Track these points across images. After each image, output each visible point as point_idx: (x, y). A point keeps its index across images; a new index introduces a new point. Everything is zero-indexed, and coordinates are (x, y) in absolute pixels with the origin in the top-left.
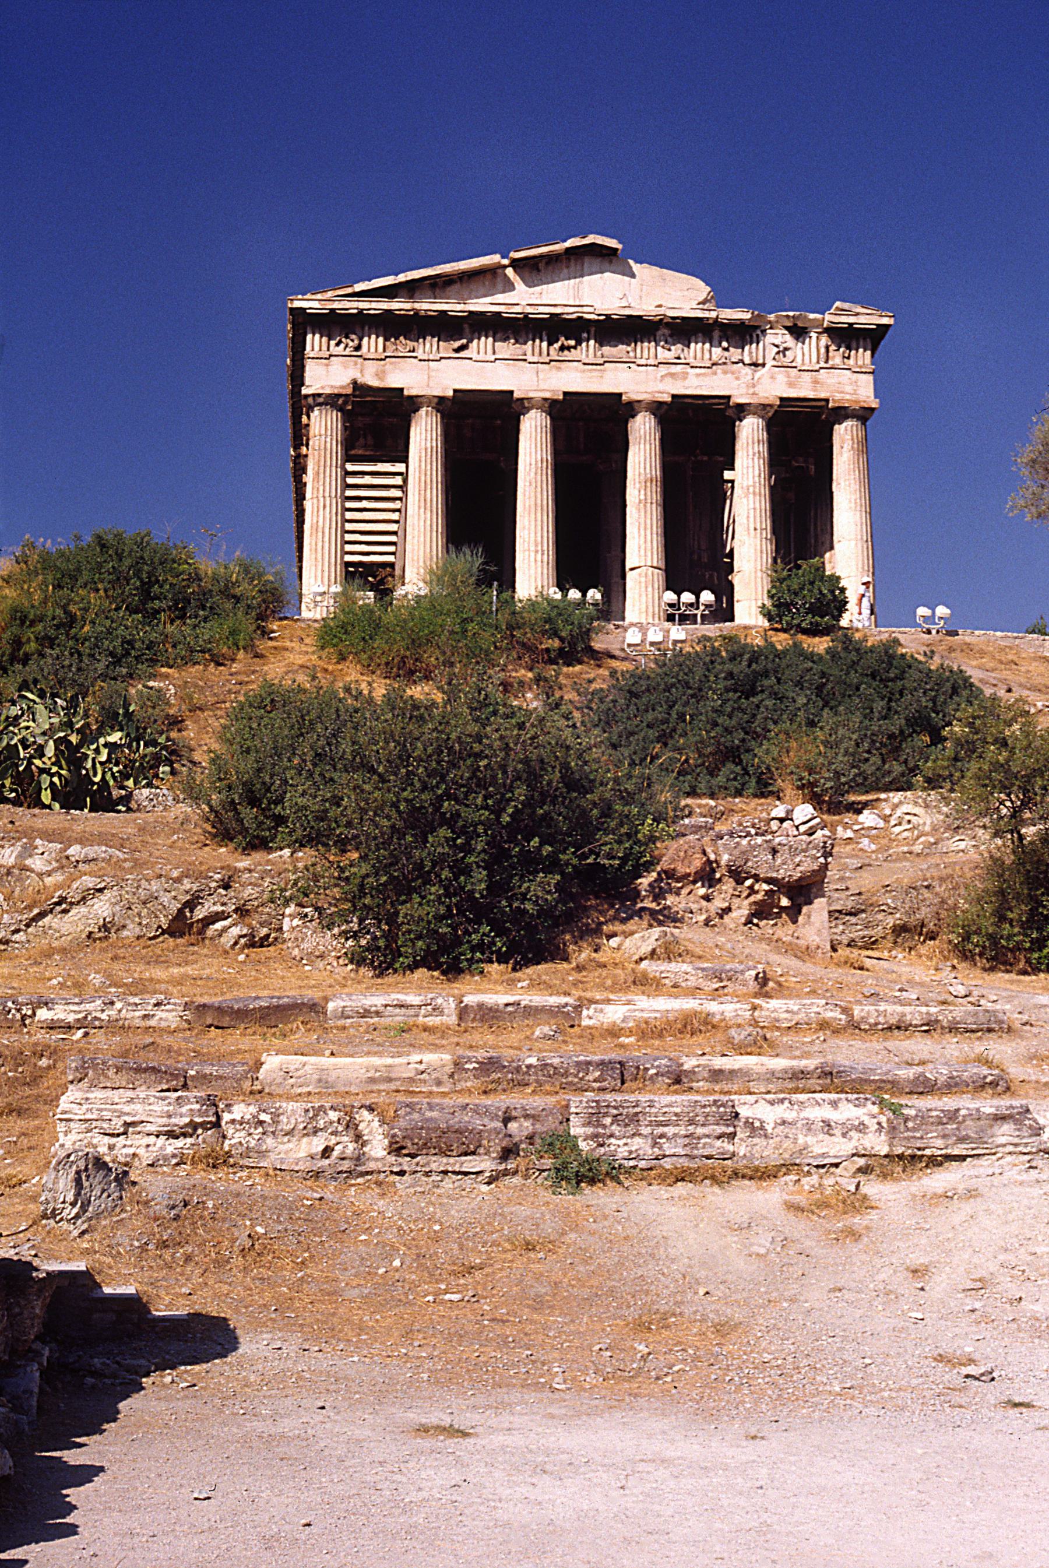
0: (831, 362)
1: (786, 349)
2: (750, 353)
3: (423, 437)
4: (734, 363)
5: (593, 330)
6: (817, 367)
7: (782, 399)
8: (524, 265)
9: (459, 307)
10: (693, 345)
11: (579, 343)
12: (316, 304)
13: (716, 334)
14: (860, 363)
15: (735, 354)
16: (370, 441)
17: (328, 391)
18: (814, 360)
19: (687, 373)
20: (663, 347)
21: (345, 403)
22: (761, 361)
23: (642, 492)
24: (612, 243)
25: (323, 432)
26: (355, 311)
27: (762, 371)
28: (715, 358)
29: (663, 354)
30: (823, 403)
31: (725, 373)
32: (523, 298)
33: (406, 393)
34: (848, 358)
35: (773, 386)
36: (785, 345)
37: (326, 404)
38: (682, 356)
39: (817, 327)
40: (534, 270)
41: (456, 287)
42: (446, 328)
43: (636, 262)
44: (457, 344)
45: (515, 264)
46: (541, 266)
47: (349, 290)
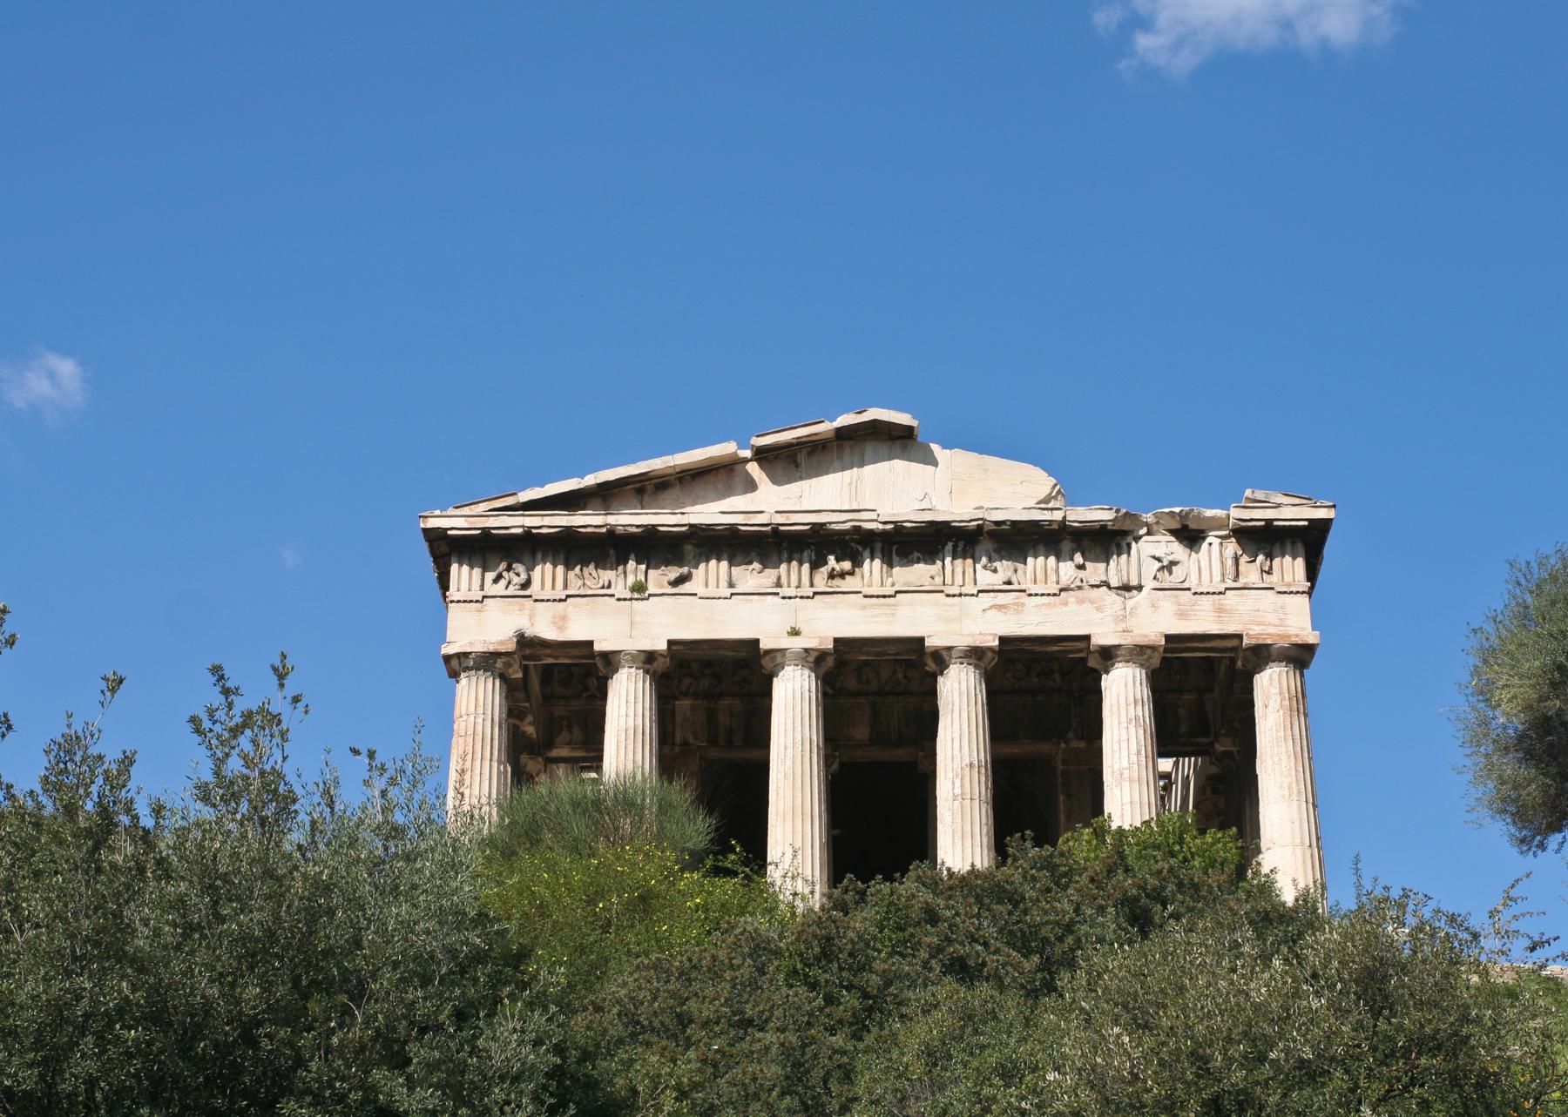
0: (1242, 581)
1: (1173, 563)
2: (1119, 571)
3: (623, 712)
4: (1093, 586)
5: (878, 546)
6: (1221, 588)
7: (1168, 638)
8: (776, 457)
9: (672, 520)
10: (1030, 560)
11: (857, 563)
12: (461, 523)
14: (1288, 578)
15: (1095, 571)
16: (577, 733)
17: (479, 648)
18: (1217, 576)
19: (1023, 605)
20: (985, 567)
21: (508, 665)
22: (1134, 583)
23: (958, 783)
24: (902, 418)
25: (472, 709)
26: (520, 531)
27: (1137, 598)
28: (1064, 581)
29: (986, 578)
30: (1234, 643)
31: (1080, 602)
32: (770, 502)
33: (597, 647)
34: (1269, 572)
35: (1155, 619)
36: (1171, 558)
37: (478, 669)
38: (1014, 580)
39: (1220, 528)
40: (788, 461)
43: (944, 447)
44: (674, 572)
45: (762, 455)
46: (802, 458)
47: (510, 501)
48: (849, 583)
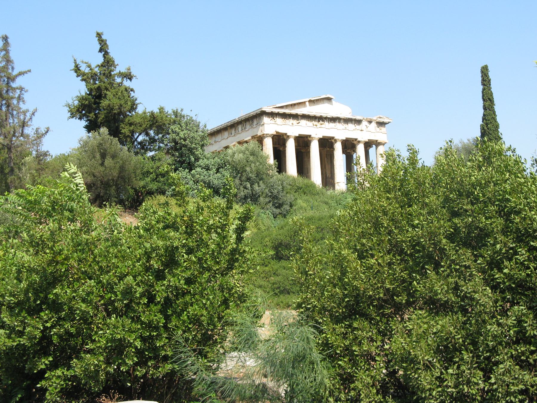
13: (353, 122)
15: (358, 127)
41: (296, 106)
42: (295, 117)
44: (298, 122)
48: (323, 126)
